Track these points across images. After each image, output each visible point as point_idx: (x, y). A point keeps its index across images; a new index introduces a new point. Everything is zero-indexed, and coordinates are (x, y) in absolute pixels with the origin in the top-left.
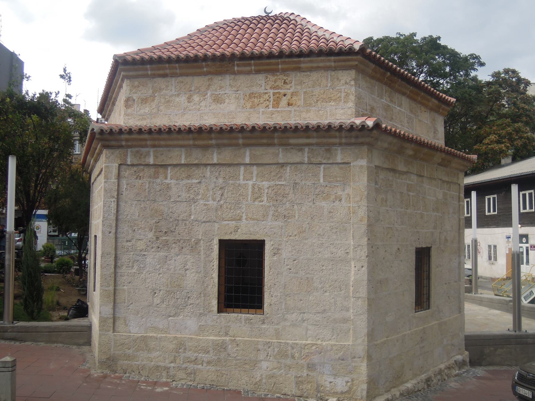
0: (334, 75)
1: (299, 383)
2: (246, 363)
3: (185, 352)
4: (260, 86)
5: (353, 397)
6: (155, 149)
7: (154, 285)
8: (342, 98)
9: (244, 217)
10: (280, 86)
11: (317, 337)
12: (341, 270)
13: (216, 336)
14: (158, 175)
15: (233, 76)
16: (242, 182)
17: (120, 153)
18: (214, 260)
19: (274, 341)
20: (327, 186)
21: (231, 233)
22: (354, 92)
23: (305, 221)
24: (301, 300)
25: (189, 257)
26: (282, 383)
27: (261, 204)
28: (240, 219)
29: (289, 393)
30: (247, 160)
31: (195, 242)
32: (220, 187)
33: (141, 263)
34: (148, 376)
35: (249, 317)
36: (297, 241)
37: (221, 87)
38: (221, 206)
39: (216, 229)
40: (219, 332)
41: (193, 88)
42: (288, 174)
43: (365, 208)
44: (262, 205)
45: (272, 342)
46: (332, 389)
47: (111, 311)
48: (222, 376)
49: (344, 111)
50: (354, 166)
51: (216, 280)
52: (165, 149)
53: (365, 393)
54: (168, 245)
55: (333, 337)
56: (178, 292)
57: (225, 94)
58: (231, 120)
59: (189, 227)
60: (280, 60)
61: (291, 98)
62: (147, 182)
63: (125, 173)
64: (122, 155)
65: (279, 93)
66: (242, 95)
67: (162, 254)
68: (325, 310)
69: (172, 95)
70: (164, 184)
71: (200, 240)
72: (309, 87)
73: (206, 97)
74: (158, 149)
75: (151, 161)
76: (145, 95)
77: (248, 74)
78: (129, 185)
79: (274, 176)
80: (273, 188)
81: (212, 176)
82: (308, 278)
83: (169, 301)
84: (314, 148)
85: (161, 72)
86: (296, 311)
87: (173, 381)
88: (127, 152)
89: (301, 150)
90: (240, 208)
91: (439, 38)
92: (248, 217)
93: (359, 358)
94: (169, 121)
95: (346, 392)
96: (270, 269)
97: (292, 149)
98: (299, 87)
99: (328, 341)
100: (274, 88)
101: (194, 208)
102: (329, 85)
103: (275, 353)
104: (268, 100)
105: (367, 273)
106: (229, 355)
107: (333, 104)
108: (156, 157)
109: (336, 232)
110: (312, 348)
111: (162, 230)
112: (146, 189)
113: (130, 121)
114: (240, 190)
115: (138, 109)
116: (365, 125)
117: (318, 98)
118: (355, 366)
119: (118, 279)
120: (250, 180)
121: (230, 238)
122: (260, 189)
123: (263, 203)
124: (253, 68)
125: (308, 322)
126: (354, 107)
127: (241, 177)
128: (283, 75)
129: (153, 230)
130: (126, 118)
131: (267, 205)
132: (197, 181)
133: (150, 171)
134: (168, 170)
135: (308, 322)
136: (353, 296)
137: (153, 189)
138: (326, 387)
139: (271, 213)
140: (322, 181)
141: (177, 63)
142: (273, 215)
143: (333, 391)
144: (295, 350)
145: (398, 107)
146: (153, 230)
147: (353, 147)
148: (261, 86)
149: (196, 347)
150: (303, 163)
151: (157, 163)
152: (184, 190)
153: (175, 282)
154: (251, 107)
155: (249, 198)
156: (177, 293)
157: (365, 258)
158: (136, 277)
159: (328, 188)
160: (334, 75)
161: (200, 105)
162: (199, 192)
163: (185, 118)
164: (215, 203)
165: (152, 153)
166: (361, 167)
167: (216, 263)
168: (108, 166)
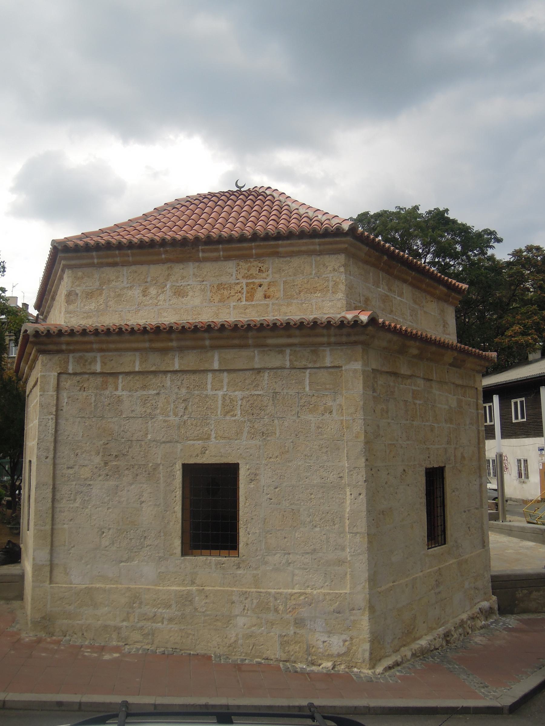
0: (320, 261)
1: (284, 644)
2: (218, 620)
3: (140, 607)
4: (230, 276)
5: (353, 660)
6: (102, 354)
7: (102, 523)
8: (330, 288)
9: (213, 435)
10: (254, 275)
11: (306, 585)
12: (334, 499)
13: (179, 585)
14: (107, 385)
15: (197, 264)
16: (210, 392)
17: (60, 359)
18: (176, 490)
19: (252, 590)
20: (314, 395)
21: (197, 455)
22: (344, 281)
23: (288, 439)
24: (285, 538)
25: (145, 486)
26: (262, 645)
27: (234, 418)
28: (208, 438)
29: (272, 657)
30: (216, 366)
31: (153, 467)
32: (182, 400)
33: (85, 495)
34: (93, 639)
35: (220, 560)
36: (279, 463)
37: (183, 277)
38: (184, 423)
39: (179, 450)
40: (184, 580)
41: (149, 279)
42: (266, 382)
43: (361, 422)
44: (235, 420)
45: (250, 592)
46: (326, 651)
47: (48, 557)
48: (188, 637)
49: (332, 303)
50: (346, 370)
51: (179, 515)
52: (115, 353)
53: (367, 655)
54: (119, 471)
55: (326, 584)
56: (132, 531)
57: (188, 285)
58: (196, 316)
59: (145, 449)
60: (253, 244)
61: (268, 289)
62: (93, 394)
63: (65, 383)
64: (63, 361)
65: (254, 283)
66: (208, 286)
67: (112, 483)
68: (315, 550)
69: (124, 288)
70: (114, 396)
71: (159, 465)
72: (290, 276)
73: (165, 289)
74: (106, 354)
75: (98, 368)
76: (91, 288)
77: (214, 261)
78: (70, 399)
79: (249, 384)
80: (247, 399)
81: (173, 385)
82: (293, 510)
83: (120, 542)
84: (297, 349)
85: (110, 260)
86: (279, 552)
87: (125, 645)
88: (68, 358)
89: (281, 352)
90: (208, 424)
92: (217, 435)
93: (359, 610)
94: (120, 319)
95: (343, 654)
96: (246, 499)
97: (271, 350)
98: (277, 276)
99: (319, 589)
100: (247, 277)
101: (151, 426)
102: (314, 272)
103: (254, 606)
105: (365, 503)
106: (196, 609)
107: (319, 295)
108: (104, 363)
109: (327, 451)
110: (300, 599)
111: (112, 454)
112: (92, 403)
113: (72, 319)
114: (207, 402)
115: (82, 305)
116: (358, 320)
117: (301, 289)
118: (354, 620)
119: (56, 516)
120: (219, 390)
121: (196, 462)
122: (232, 400)
123: (236, 417)
124: (221, 253)
125: (294, 566)
126: (344, 298)
127: (209, 386)
128: (258, 261)
129: (101, 454)
130: (67, 315)
131: (241, 419)
132: (155, 392)
133: (96, 381)
134: (118, 380)
135: (294, 566)
136: (350, 532)
137: (101, 403)
138: (318, 648)
139: (246, 429)
140: (307, 389)
141: (129, 249)
142: (249, 432)
143: (327, 653)
144: (278, 602)
145: (398, 297)
146: (101, 454)
147: (345, 347)
148: (232, 275)
149: (155, 600)
150: (285, 368)
151: (105, 371)
152: (138, 404)
153: (127, 518)
154: (220, 301)
155: (219, 413)
156: (130, 531)
157: (363, 483)
158: (80, 513)
159: (315, 398)
160: (320, 261)
161: (158, 299)
162: (158, 405)
163: (139, 315)
164: (177, 419)
165: (98, 359)
166: (355, 371)
168: (45, 375)
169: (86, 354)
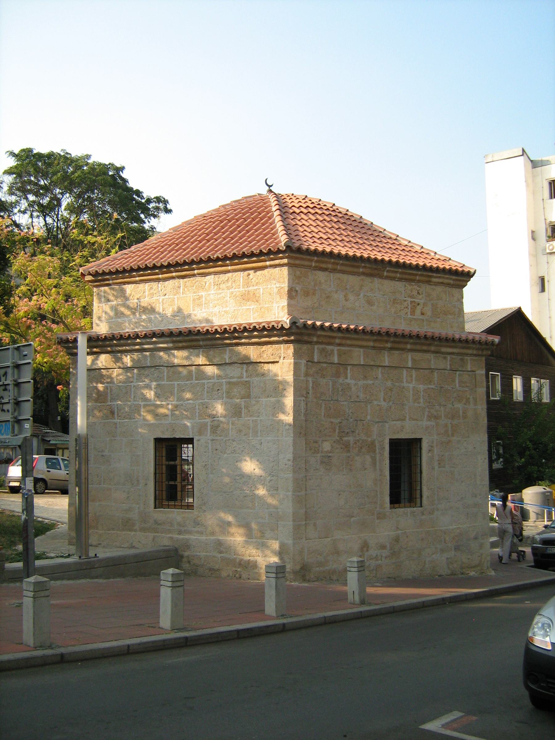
6: (339, 348)
9: (408, 417)
15: (380, 280)
16: (405, 384)
28: (404, 420)
29: (443, 574)
57: (375, 296)
66: (387, 299)
68: (462, 498)
89: (445, 358)
91: (122, 169)
104: (407, 308)
132: (372, 382)
139: (426, 413)
142: (428, 416)
167: (387, 462)
169: (327, 347)
